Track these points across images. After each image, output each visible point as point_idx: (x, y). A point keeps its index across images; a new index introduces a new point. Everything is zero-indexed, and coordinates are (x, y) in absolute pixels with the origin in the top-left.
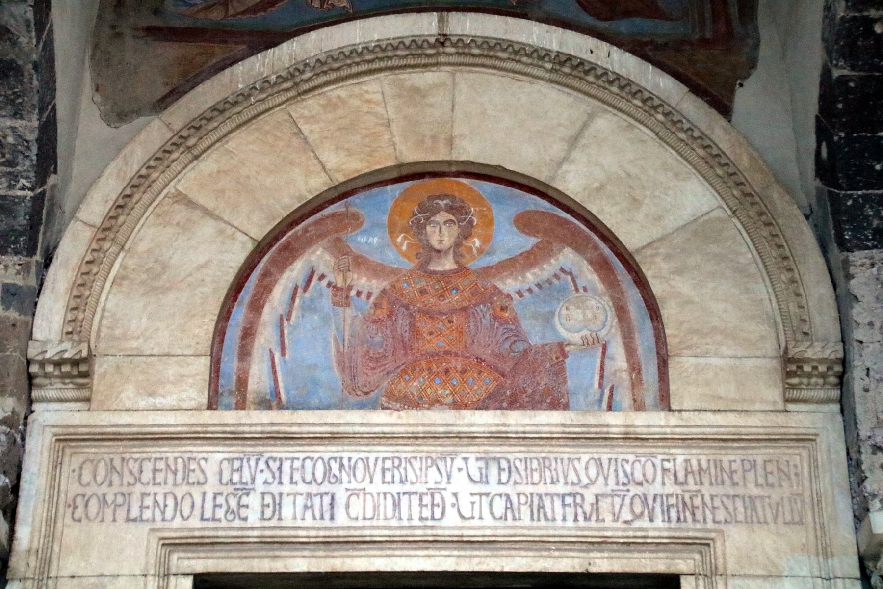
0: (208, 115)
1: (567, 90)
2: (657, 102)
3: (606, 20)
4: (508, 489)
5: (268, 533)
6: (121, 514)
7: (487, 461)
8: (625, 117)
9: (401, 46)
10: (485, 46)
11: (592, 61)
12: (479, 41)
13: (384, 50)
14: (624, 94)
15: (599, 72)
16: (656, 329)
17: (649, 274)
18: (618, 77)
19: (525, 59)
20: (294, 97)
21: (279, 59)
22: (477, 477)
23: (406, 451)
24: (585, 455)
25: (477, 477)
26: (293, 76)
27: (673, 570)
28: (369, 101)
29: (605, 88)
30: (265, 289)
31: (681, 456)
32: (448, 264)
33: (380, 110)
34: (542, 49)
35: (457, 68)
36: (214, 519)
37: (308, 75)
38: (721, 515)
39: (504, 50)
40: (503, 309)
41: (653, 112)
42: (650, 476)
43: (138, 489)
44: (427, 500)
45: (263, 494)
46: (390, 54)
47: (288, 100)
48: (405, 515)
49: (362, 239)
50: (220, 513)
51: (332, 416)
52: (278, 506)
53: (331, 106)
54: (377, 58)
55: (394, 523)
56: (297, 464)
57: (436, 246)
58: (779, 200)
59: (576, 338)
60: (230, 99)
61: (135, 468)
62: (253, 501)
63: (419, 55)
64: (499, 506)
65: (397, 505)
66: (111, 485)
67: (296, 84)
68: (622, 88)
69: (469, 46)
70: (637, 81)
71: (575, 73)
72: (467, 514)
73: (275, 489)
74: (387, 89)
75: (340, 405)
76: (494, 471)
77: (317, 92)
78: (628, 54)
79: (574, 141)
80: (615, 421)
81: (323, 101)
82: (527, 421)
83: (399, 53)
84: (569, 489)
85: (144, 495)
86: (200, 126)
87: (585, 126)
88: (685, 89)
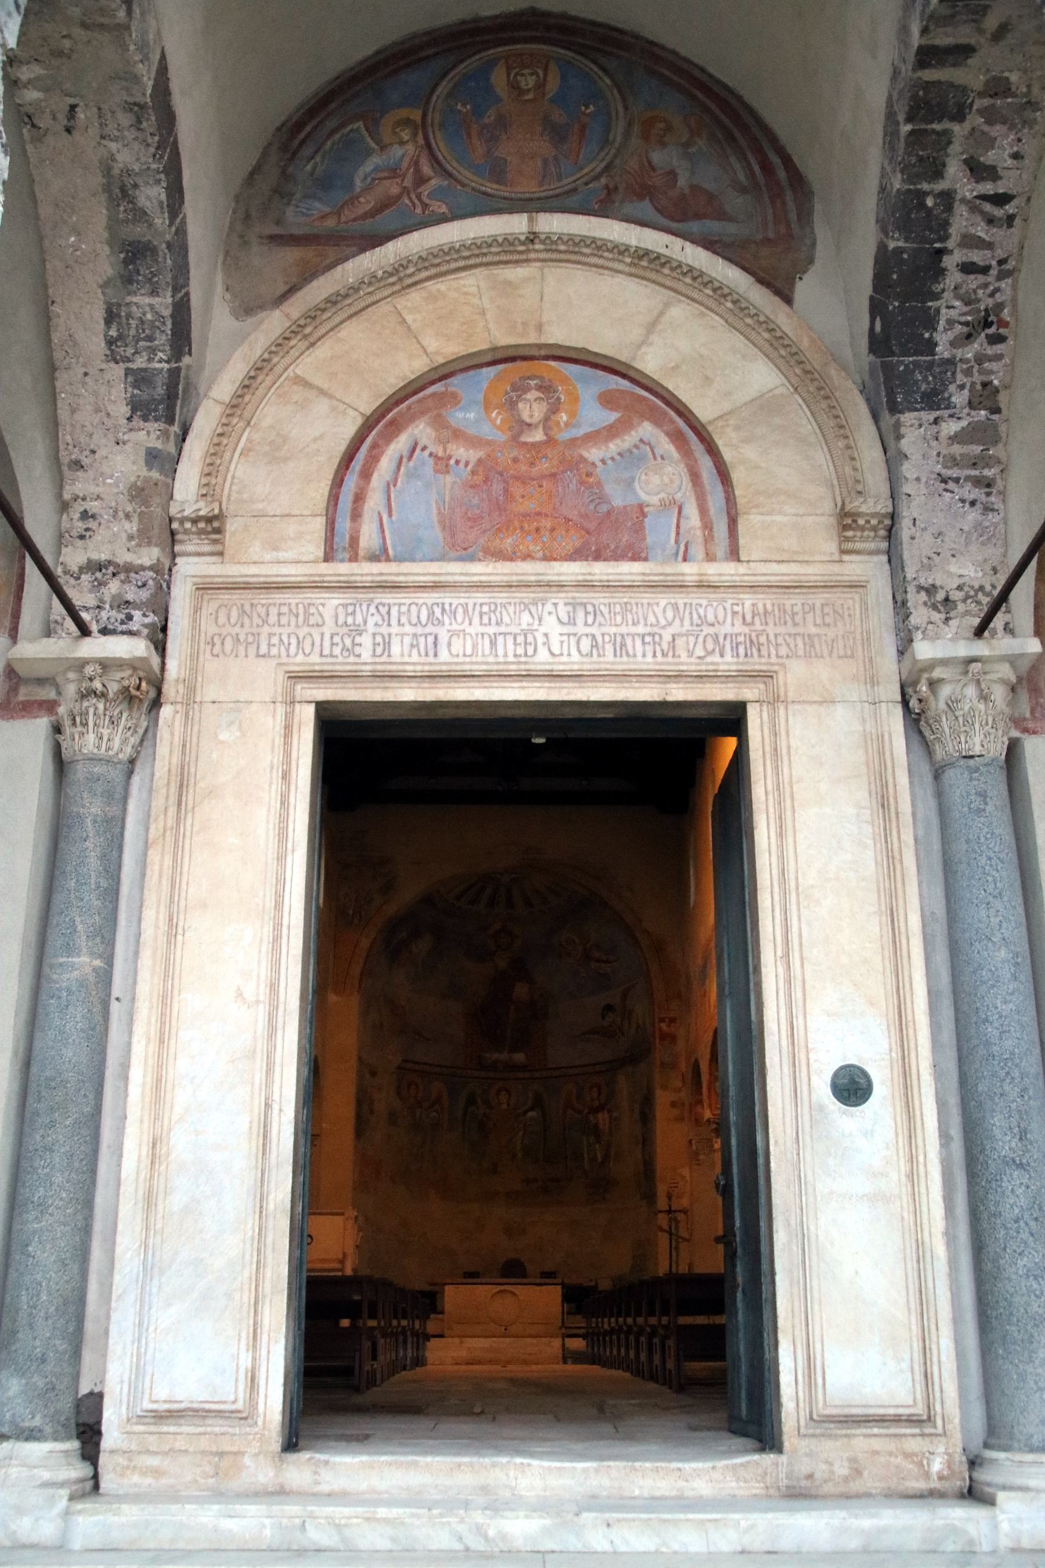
0: (322, 306)
1: (645, 282)
2: (726, 291)
3: (679, 221)
4: (594, 630)
5: (379, 667)
6: (252, 651)
7: (574, 606)
8: (696, 305)
9: (495, 243)
10: (570, 243)
11: (668, 254)
12: (565, 238)
13: (479, 247)
14: (696, 285)
15: (675, 264)
16: (726, 492)
17: (720, 443)
18: (691, 269)
19: (606, 254)
20: (399, 291)
21: (385, 256)
22: (565, 620)
23: (501, 597)
24: (663, 600)
25: (565, 620)
26: (397, 271)
27: (740, 698)
28: (466, 294)
29: (679, 280)
30: (373, 459)
31: (748, 600)
32: (538, 436)
33: (475, 301)
34: (622, 244)
35: (544, 264)
36: (332, 656)
37: (411, 270)
38: (783, 651)
39: (588, 246)
40: (589, 475)
41: (722, 300)
42: (721, 618)
43: (266, 630)
44: (520, 639)
45: (374, 635)
46: (485, 251)
47: (393, 293)
48: (501, 651)
49: (460, 415)
50: (337, 651)
51: (434, 567)
52: (387, 644)
53: (432, 298)
54: (473, 255)
55: (491, 659)
56: (404, 609)
57: (528, 420)
58: (834, 372)
59: (654, 500)
60: (342, 292)
61: (262, 611)
62: (366, 640)
63: (511, 252)
64: (586, 644)
65: (493, 644)
66: (242, 626)
67: (400, 279)
68: (694, 279)
69: (555, 243)
70: (709, 272)
71: (652, 266)
72: (557, 651)
73: (384, 630)
74: (482, 284)
75: (442, 558)
76: (580, 614)
77: (419, 287)
78: (700, 249)
79: (651, 327)
80: (690, 570)
81: (424, 294)
82: (611, 571)
83: (493, 250)
84: (648, 630)
85: (270, 635)
86: (315, 316)
87: (661, 314)
88: (752, 279)
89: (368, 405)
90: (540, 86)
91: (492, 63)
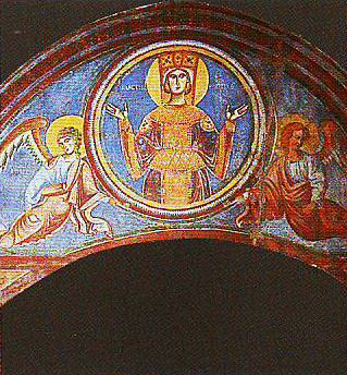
90: (191, 89)
91: (146, 63)
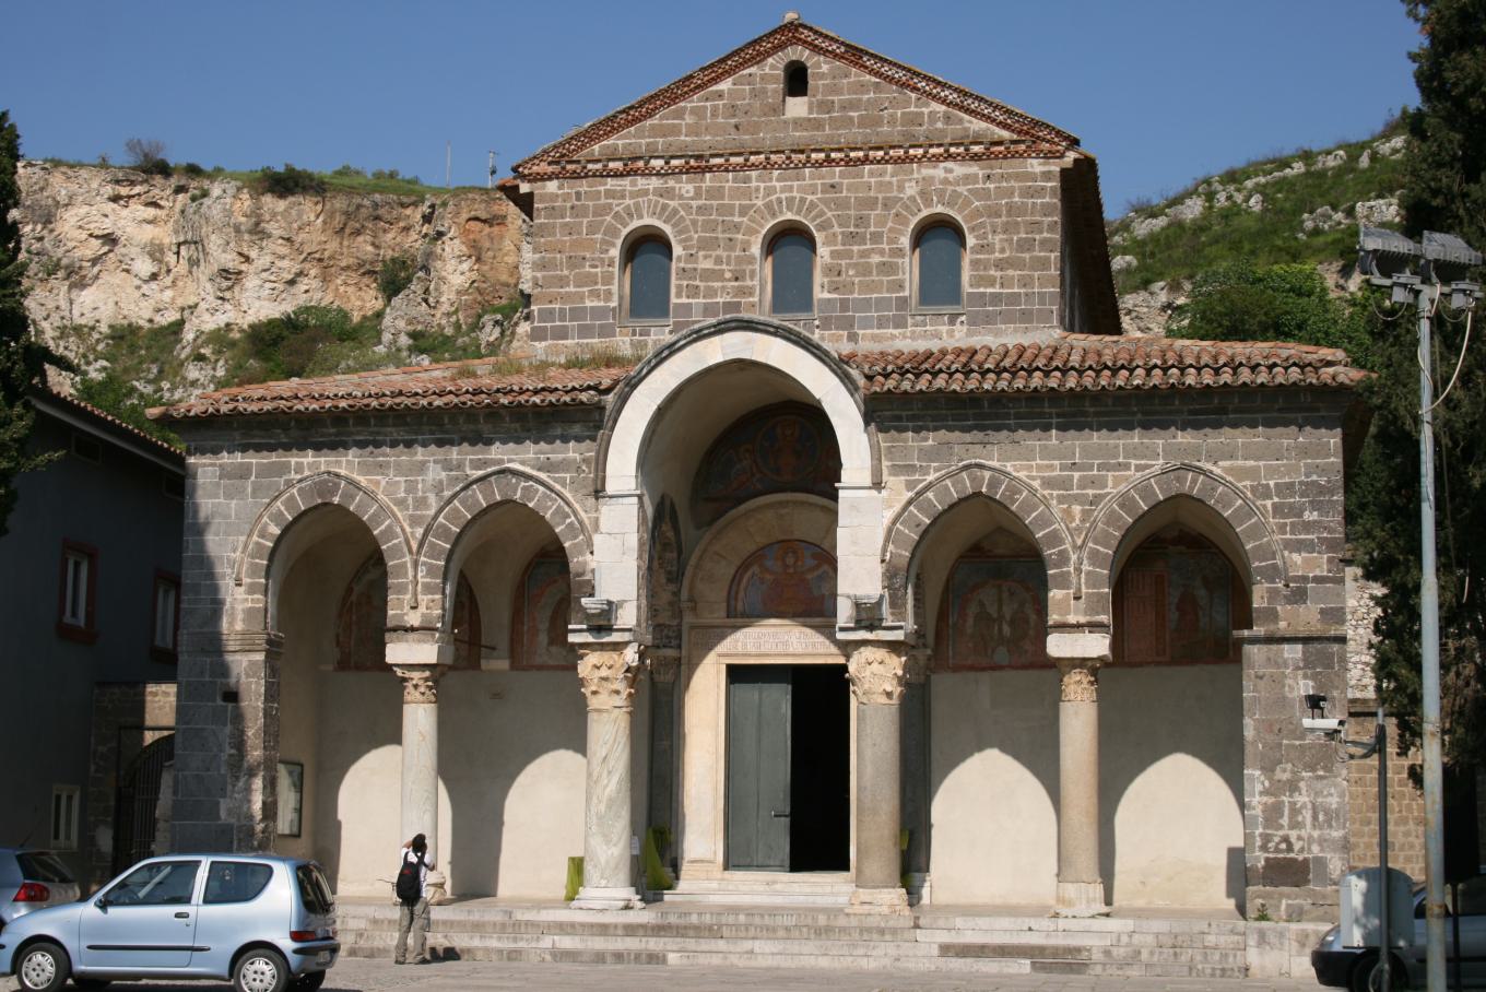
32: (791, 571)
89: (738, 563)
